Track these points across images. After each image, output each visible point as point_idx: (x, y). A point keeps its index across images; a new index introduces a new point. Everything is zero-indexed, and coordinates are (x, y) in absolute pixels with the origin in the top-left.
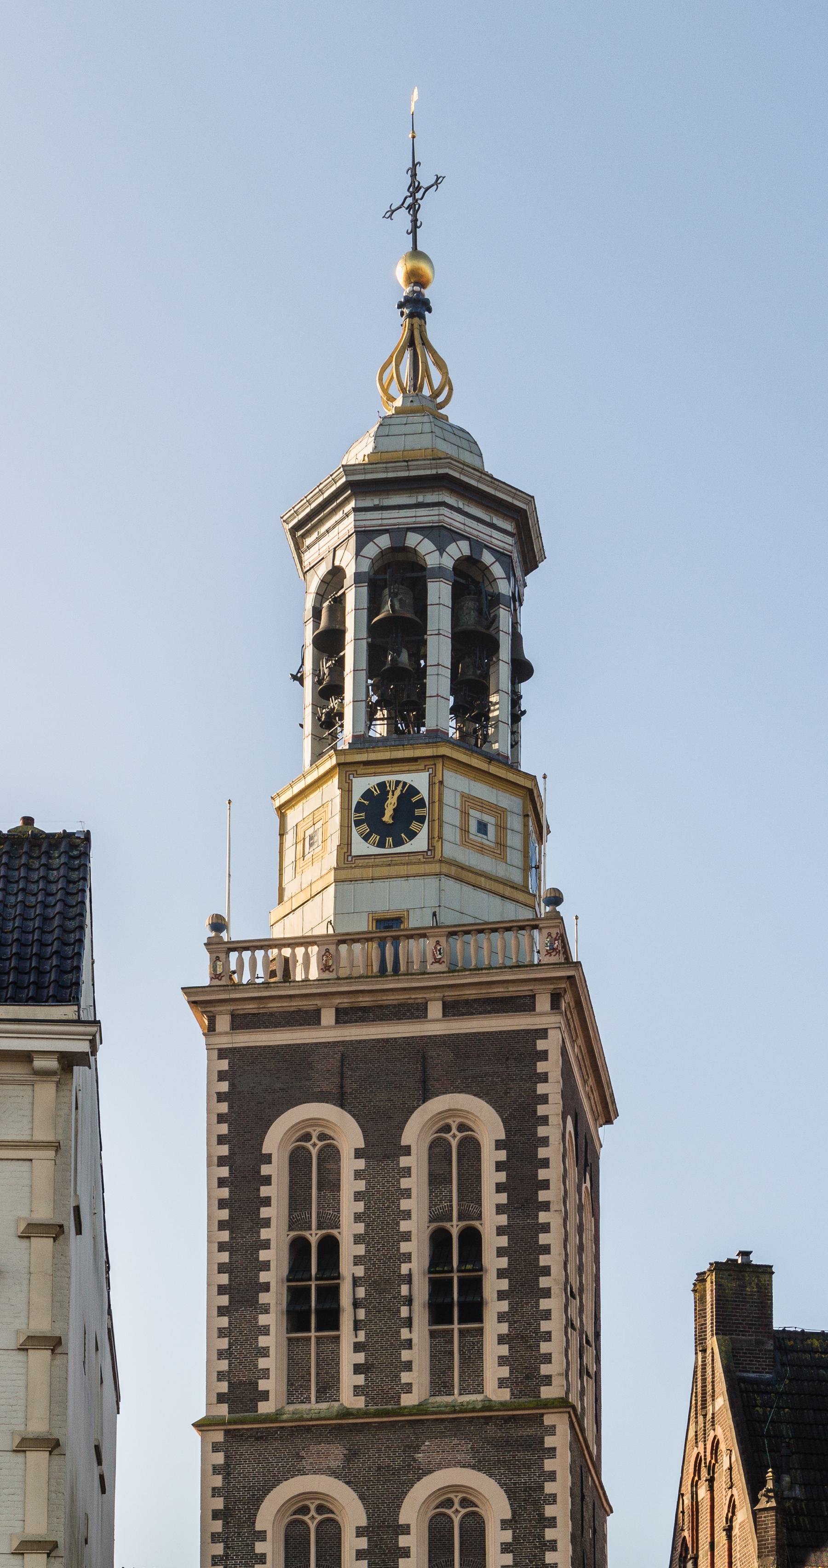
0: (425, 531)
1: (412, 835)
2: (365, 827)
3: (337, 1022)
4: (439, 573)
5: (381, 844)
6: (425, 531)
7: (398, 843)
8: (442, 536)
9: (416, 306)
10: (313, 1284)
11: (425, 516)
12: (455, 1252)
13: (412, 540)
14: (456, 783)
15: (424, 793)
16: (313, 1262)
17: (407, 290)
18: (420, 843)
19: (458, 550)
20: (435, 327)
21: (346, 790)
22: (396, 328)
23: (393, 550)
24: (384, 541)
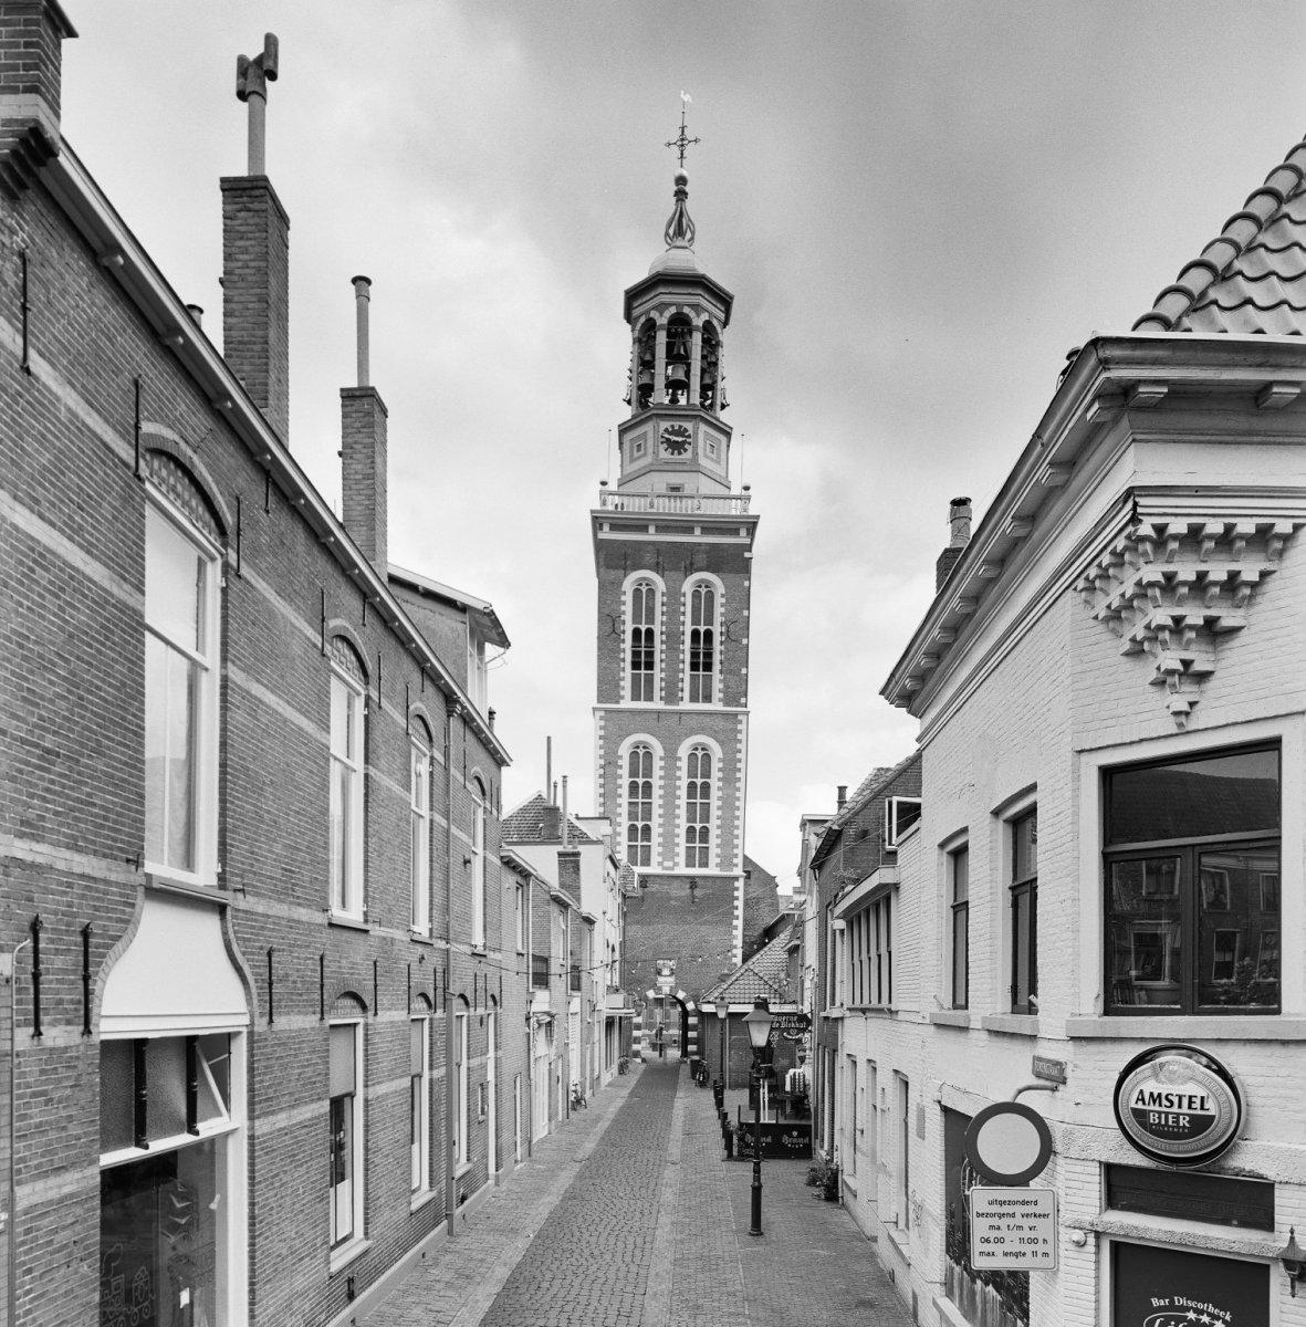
0: (691, 306)
1: (686, 450)
2: (665, 446)
3: (656, 531)
4: (697, 328)
5: (672, 454)
6: (691, 306)
7: (680, 453)
8: (697, 308)
9: (681, 195)
10: (643, 649)
11: (693, 300)
12: (703, 640)
13: (686, 310)
14: (703, 427)
15: (690, 432)
16: (643, 638)
17: (675, 188)
18: (687, 456)
19: (705, 317)
20: (689, 205)
21: (656, 431)
22: (670, 204)
23: (677, 313)
24: (673, 310)
